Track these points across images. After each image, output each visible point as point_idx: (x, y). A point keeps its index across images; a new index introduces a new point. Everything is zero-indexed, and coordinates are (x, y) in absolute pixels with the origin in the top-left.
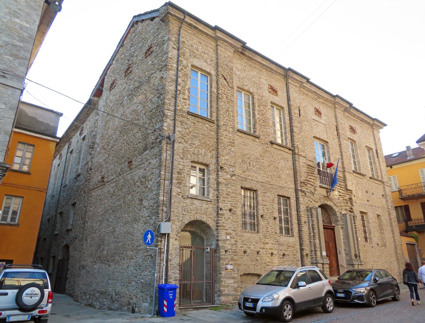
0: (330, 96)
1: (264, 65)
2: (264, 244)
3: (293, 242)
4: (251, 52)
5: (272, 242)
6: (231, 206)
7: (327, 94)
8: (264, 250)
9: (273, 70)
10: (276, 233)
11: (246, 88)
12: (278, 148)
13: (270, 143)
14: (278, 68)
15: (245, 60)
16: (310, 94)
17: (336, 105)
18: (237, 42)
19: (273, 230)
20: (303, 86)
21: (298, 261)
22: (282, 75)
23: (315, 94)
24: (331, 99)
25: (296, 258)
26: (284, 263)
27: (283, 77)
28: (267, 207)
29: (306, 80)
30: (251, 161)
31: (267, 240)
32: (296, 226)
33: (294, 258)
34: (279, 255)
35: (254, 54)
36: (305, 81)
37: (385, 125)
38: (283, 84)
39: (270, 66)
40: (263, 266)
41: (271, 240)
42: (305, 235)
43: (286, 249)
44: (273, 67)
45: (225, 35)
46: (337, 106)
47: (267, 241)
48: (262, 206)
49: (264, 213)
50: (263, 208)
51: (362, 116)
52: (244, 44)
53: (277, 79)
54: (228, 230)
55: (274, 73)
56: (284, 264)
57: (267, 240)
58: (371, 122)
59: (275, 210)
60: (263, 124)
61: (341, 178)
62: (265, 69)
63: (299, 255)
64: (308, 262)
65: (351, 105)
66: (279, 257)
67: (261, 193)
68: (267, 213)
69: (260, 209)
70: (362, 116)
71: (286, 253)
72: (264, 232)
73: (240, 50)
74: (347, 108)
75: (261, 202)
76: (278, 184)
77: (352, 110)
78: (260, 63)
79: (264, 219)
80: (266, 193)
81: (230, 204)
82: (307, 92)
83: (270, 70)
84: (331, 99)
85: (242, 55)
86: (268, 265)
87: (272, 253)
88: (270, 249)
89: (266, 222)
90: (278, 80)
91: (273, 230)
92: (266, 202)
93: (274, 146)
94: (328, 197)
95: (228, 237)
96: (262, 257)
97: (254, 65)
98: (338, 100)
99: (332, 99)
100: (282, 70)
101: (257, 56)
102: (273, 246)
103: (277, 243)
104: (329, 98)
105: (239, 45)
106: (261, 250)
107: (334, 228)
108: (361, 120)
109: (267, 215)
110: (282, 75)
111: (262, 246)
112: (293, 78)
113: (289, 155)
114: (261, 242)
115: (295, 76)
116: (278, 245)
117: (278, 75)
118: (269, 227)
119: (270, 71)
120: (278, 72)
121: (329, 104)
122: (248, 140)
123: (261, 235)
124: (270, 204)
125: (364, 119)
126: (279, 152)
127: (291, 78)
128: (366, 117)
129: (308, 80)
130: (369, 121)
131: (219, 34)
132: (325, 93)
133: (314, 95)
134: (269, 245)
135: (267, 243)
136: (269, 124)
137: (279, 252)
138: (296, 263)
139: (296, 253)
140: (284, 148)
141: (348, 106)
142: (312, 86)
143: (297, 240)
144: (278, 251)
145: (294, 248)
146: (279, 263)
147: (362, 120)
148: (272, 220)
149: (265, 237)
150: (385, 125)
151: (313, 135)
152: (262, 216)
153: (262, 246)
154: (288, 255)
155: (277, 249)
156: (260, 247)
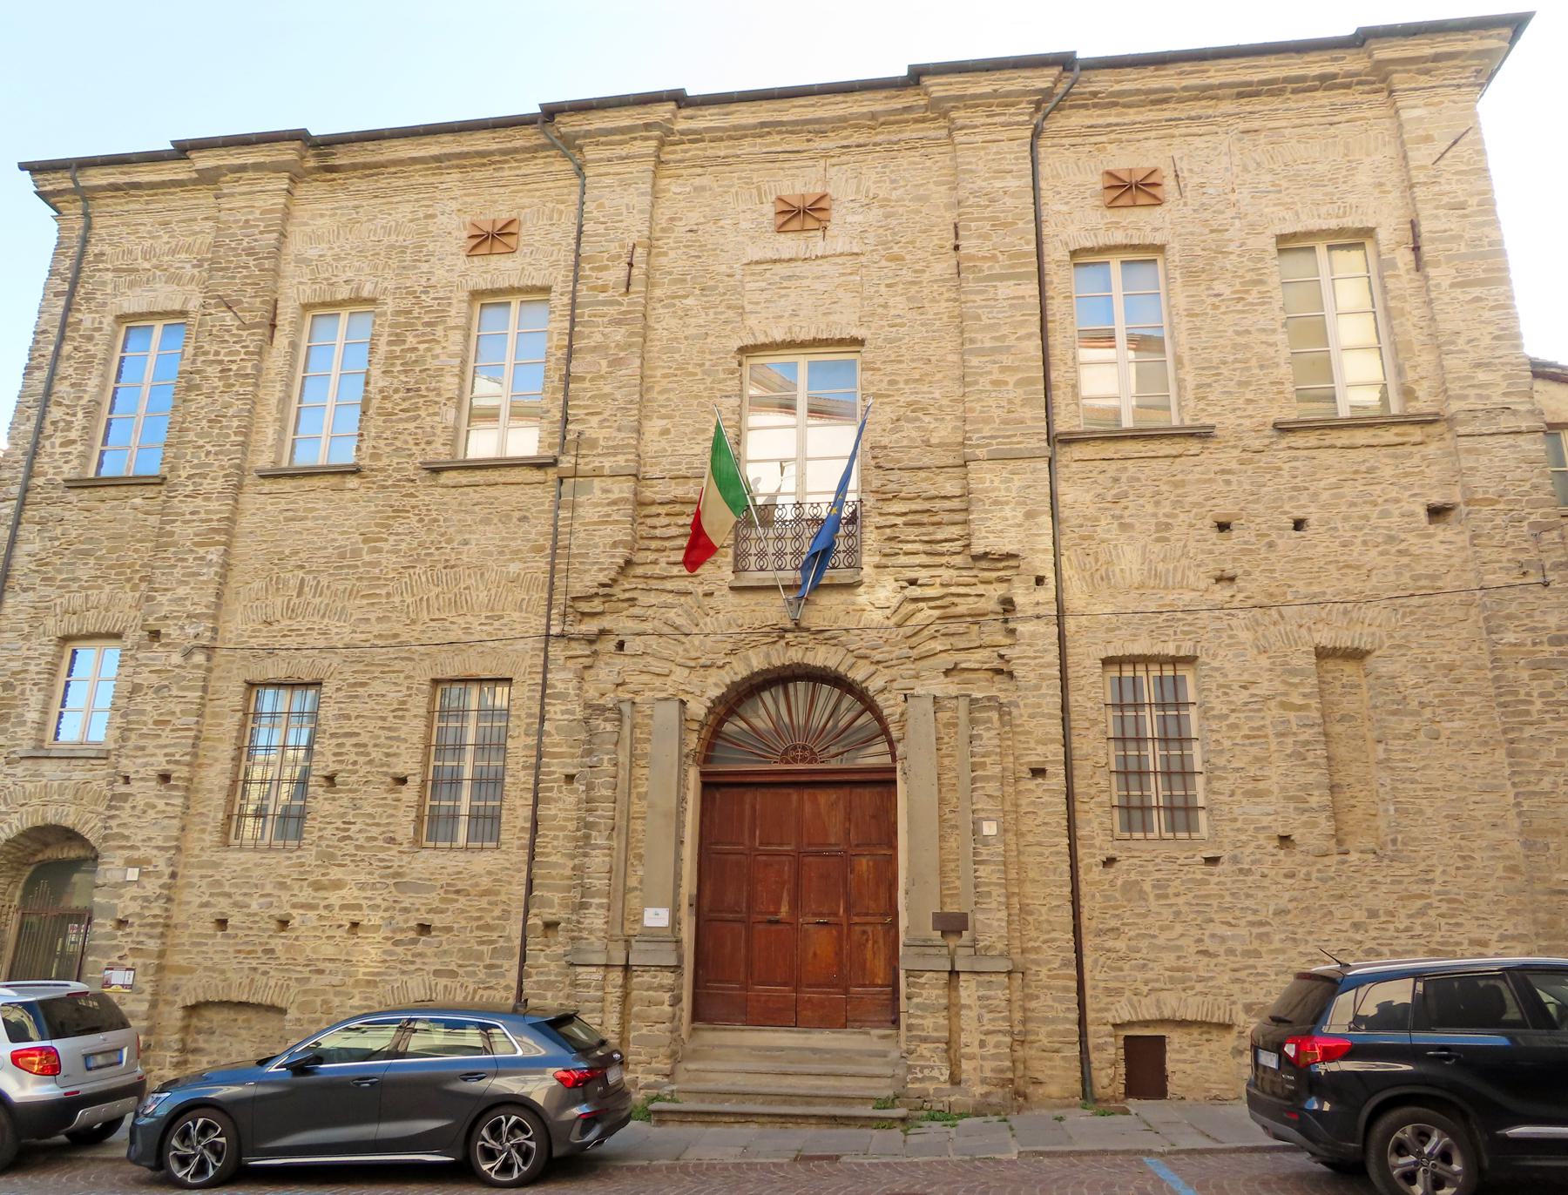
0: (882, 94)
1: (437, 159)
2: (317, 886)
3: (489, 873)
4: (356, 147)
5: (363, 878)
6: (168, 762)
7: (857, 96)
8: (312, 914)
9: (491, 153)
10: (392, 840)
11: (343, 293)
12: (464, 481)
13: (424, 473)
14: (502, 133)
15: (357, 184)
16: (747, 147)
17: (953, 114)
18: (278, 146)
19: (375, 831)
20: (682, 133)
21: (508, 953)
22: (543, 147)
23: (779, 133)
24: (898, 104)
25: (492, 942)
26: (412, 963)
27: (552, 153)
28: (364, 738)
29: (672, 106)
30: (309, 572)
31: (336, 873)
32: (519, 802)
33: (482, 943)
34: (394, 931)
35: (370, 145)
36: (664, 111)
37: (1515, 24)
38: (561, 183)
39: (465, 149)
40: (294, 976)
41: (357, 873)
42: (556, 838)
43: (436, 904)
44: (482, 142)
45: (222, 151)
46: (960, 116)
47: (340, 876)
48: (334, 741)
49: (338, 767)
50: (338, 745)
51: (1217, 74)
52: (300, 136)
53: (521, 180)
54: (138, 848)
55: (506, 162)
56: (412, 967)
57: (336, 873)
58: (1353, 63)
59: (403, 746)
60: (405, 405)
61: (955, 504)
62: (457, 166)
63: (515, 929)
64: (546, 957)
65: (1065, 62)
66: (387, 939)
67: (338, 690)
68: (355, 763)
69: (322, 754)
70: (1217, 74)
71: (436, 921)
72: (324, 843)
73: (311, 163)
74: (1047, 93)
75: (332, 723)
76: (442, 634)
77: (1103, 82)
78: (414, 161)
79: (340, 791)
80: (363, 685)
81: (166, 755)
82: (721, 150)
83: (478, 160)
84: (898, 104)
85: (335, 175)
86: (321, 972)
87: (355, 925)
88: (343, 907)
89: (345, 801)
90: (529, 180)
91: (375, 831)
92: (357, 723)
93: (446, 478)
94: (798, 627)
95: (133, 874)
96: (297, 938)
97: (401, 183)
98: (937, 87)
99: (908, 98)
100: (530, 130)
101: (386, 144)
102: (369, 894)
103: (391, 881)
104: (878, 107)
105: (287, 153)
106: (294, 912)
107: (887, 776)
108: (1240, 95)
109: (356, 772)
110: (543, 147)
111: (305, 895)
112: (588, 134)
113: (539, 491)
114: (305, 884)
115: (598, 122)
116: (392, 889)
117: (526, 160)
118: (359, 820)
119: (484, 165)
120: (516, 151)
121: (911, 132)
122: (312, 495)
123: (310, 856)
124: (380, 723)
125: (1256, 78)
126: (474, 495)
127: (585, 137)
128: (1273, 60)
129: (679, 99)
130: (1315, 70)
131: (205, 161)
132: (840, 98)
133: (777, 138)
134: (343, 892)
135: (338, 885)
136: (439, 395)
137: (392, 918)
138: (488, 962)
139: (499, 918)
140: (503, 471)
141: (1042, 80)
142: (733, 107)
143: (515, 859)
144: (386, 915)
145: (493, 898)
146: (385, 961)
147: (1246, 92)
148: (378, 791)
149: (327, 858)
150: (1515, 24)
151: (737, 344)
152: (330, 779)
153: (305, 895)
154: (448, 929)
155: (384, 905)
156: (295, 900)
